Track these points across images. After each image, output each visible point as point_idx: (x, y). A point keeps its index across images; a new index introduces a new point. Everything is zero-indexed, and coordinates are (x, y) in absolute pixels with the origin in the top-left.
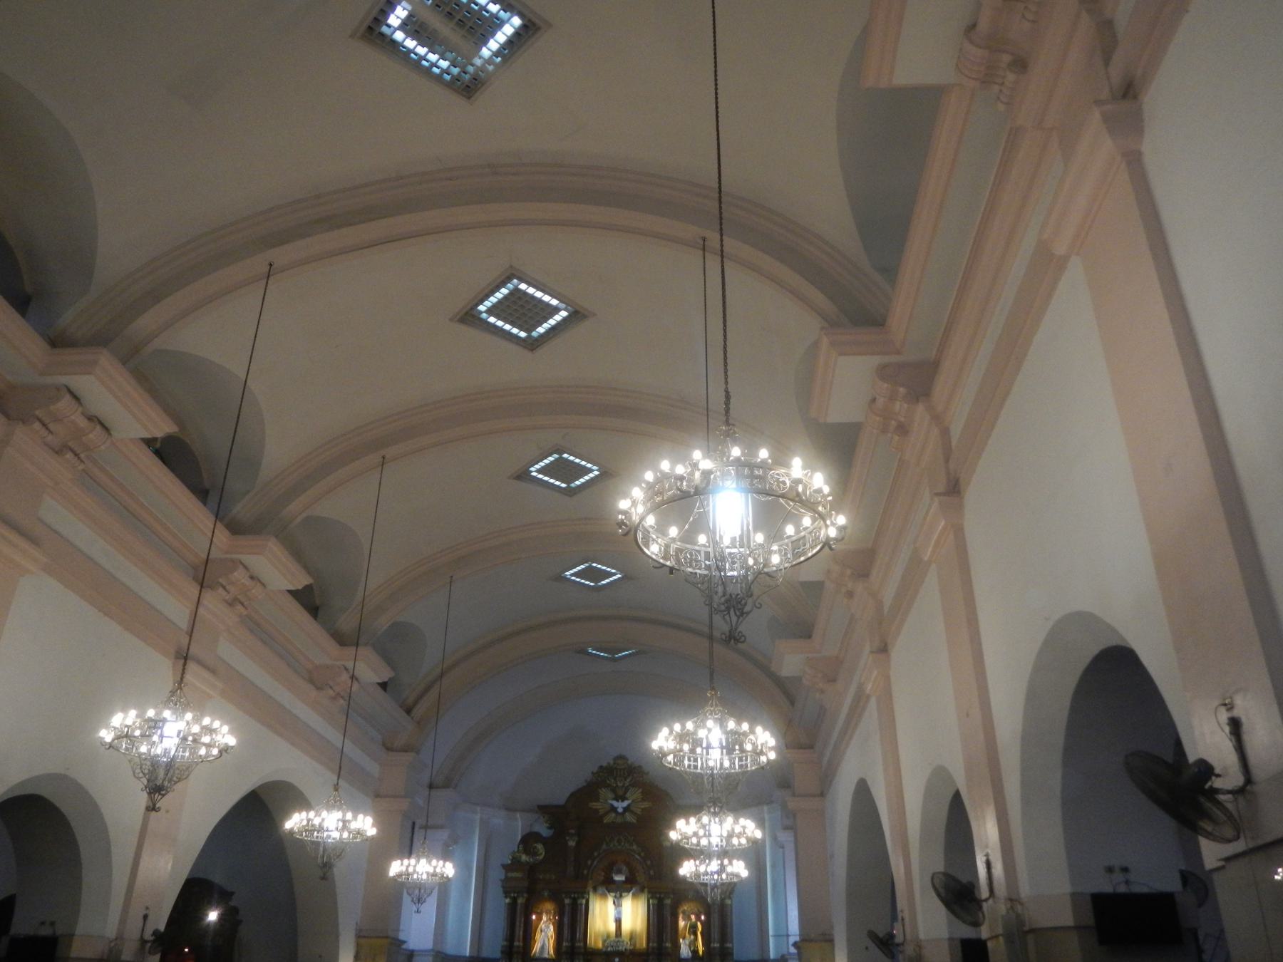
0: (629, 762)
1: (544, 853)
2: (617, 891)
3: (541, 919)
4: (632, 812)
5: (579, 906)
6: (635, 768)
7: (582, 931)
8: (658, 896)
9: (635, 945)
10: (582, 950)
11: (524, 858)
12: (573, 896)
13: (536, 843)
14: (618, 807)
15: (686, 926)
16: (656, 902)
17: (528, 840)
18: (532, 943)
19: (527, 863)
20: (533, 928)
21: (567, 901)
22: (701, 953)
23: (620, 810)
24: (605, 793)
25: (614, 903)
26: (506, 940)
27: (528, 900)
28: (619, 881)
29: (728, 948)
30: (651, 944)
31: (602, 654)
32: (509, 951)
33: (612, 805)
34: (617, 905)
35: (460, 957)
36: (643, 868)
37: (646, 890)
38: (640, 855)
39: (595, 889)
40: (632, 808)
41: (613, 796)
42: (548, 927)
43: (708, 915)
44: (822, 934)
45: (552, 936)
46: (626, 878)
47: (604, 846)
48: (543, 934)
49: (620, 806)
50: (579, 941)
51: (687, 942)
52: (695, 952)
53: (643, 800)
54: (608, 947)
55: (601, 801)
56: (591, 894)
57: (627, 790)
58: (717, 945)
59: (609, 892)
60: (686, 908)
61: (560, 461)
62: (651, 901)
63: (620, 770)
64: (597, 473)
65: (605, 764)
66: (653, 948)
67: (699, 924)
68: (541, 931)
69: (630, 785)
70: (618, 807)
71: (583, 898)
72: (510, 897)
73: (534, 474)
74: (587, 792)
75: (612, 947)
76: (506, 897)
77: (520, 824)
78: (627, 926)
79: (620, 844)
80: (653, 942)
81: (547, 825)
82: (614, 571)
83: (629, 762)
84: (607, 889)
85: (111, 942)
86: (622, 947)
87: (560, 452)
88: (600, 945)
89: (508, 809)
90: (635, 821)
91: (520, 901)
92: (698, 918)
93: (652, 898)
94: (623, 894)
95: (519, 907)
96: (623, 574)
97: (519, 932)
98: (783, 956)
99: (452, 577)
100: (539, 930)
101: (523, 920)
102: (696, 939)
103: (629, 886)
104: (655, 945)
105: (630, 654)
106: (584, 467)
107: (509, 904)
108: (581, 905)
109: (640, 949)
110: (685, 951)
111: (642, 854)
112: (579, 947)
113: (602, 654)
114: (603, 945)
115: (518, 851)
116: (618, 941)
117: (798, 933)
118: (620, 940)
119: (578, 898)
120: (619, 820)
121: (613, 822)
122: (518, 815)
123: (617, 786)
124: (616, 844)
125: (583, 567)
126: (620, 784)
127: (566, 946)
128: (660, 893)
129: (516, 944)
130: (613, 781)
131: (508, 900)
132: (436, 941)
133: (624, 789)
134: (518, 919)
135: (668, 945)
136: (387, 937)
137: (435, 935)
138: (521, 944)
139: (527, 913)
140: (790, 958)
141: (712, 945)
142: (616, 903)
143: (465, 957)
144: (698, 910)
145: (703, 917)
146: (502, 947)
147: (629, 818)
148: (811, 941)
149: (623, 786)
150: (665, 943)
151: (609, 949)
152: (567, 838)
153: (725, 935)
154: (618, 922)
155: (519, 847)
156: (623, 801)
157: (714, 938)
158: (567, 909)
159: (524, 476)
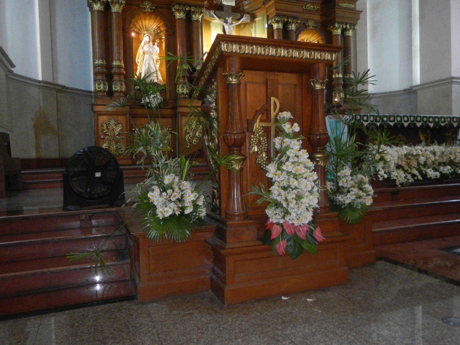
5: (195, 24)
8: (286, 20)
16: (281, 26)
20: (134, 50)
21: (179, 15)
26: (102, 58)
48: (147, 56)
58: (341, 76)
59: (219, 17)
62: (275, 26)
91: (115, 9)
93: (277, 22)
97: (117, 50)
100: (140, 51)
119: (194, 12)
138: (123, 65)
139: (125, 32)
143: (40, 82)
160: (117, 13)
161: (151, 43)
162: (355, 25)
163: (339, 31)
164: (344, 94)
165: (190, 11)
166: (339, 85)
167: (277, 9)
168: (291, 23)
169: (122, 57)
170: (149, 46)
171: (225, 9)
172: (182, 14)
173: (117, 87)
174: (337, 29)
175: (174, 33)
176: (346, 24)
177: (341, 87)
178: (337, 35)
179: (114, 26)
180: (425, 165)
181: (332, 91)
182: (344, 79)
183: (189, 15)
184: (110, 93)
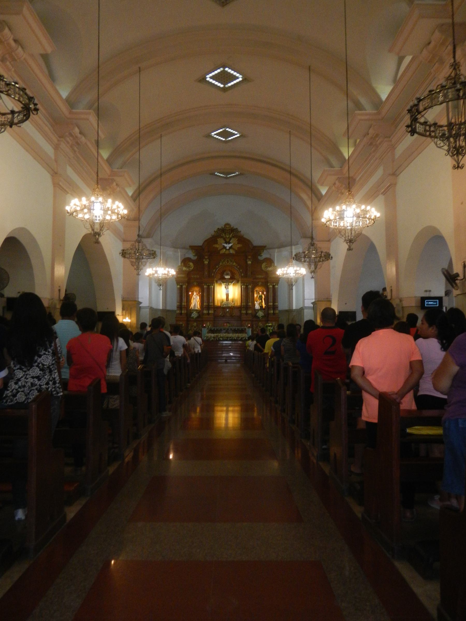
0: (232, 227)
1: (193, 267)
2: (228, 282)
3: (193, 294)
4: (234, 249)
5: (211, 289)
6: (234, 229)
7: (212, 298)
8: (246, 284)
9: (234, 304)
10: (213, 306)
11: (184, 269)
12: (208, 284)
13: (190, 262)
14: (226, 247)
15: (257, 296)
17: (185, 261)
18: (190, 303)
19: (185, 271)
20: (190, 298)
21: (205, 287)
22: (264, 307)
23: (228, 248)
24: (220, 241)
25: (225, 287)
26: (179, 302)
27: (187, 286)
28: (228, 278)
29: (276, 305)
30: (243, 304)
31: (221, 175)
32: (180, 307)
33: (224, 246)
34: (227, 288)
35: (158, 309)
36: (238, 272)
37: (240, 282)
38: (237, 267)
39: (217, 282)
40: (233, 247)
41: (224, 242)
42: (197, 297)
43: (268, 292)
44: (327, 298)
45: (198, 301)
46: (230, 277)
47: (221, 264)
49: (228, 246)
50: (211, 303)
51: (258, 303)
52: (261, 307)
53: (238, 243)
54: (223, 305)
55: (219, 244)
56: (215, 284)
57: (230, 239)
58: (271, 304)
59: (223, 283)
60: (257, 289)
61: (224, 72)
62: (242, 286)
63: (228, 230)
64: (241, 79)
65: (220, 227)
66: (244, 305)
67: (263, 296)
68: (194, 299)
69: (232, 237)
70: (226, 247)
71: (212, 285)
72: (180, 285)
73: (208, 79)
74: (212, 240)
75: (225, 305)
76: (178, 285)
77: (180, 254)
78: (230, 297)
79: (228, 263)
80: (244, 303)
81: (194, 254)
82: (236, 133)
83: (232, 227)
84: (222, 282)
85: (50, 300)
86: (230, 305)
87: (224, 67)
88: (219, 305)
89: (174, 247)
90: (235, 253)
91: (184, 286)
92: (263, 293)
93: (243, 285)
94: (230, 284)
95: (184, 289)
96: (241, 134)
97: (184, 300)
98: (302, 308)
99: (161, 134)
100: (193, 298)
101: (186, 294)
102: (262, 302)
103: (231, 280)
104: (245, 304)
105: (235, 175)
106: (235, 76)
107: (179, 288)
108: (212, 288)
109: (237, 306)
110: (257, 306)
111: (238, 267)
112: (211, 305)
113: (221, 175)
114: (221, 305)
115: (181, 266)
116: (228, 303)
117: (314, 297)
118: (229, 302)
119: (210, 285)
120: (227, 252)
121: (224, 253)
122: (179, 250)
123: (226, 237)
124: (227, 263)
125: (221, 130)
126: (228, 236)
127: (206, 305)
128: (247, 283)
129: (183, 304)
130: (224, 235)
131: (178, 286)
132: (149, 303)
133: (229, 238)
134: (184, 294)
135: (250, 304)
136: (136, 301)
137: (149, 300)
138: (186, 304)
140: (305, 309)
141: (269, 304)
142: (226, 286)
143: (160, 309)
144: (263, 290)
145: (265, 293)
146: (177, 305)
147: (232, 251)
148: (321, 301)
149: (229, 237)
150: (249, 303)
151: (224, 306)
152: (204, 260)
153: (275, 300)
154: (227, 295)
155: (181, 264)
156: (229, 243)
157: (270, 301)
158: (205, 290)
159: (203, 80)
160: (185, 288)
161: (197, 295)
162: (278, 283)
163: (271, 286)
165: (208, 285)
167: (241, 280)
168: (249, 285)
169: (185, 302)
170: (195, 297)
171: (226, 279)
172: (206, 286)
173: (183, 312)
174: (270, 285)
175: (204, 292)
176: (274, 283)
178: (270, 288)
179: (183, 291)
180: (220, 337)
182: (274, 305)
183: (209, 286)
184: (181, 314)
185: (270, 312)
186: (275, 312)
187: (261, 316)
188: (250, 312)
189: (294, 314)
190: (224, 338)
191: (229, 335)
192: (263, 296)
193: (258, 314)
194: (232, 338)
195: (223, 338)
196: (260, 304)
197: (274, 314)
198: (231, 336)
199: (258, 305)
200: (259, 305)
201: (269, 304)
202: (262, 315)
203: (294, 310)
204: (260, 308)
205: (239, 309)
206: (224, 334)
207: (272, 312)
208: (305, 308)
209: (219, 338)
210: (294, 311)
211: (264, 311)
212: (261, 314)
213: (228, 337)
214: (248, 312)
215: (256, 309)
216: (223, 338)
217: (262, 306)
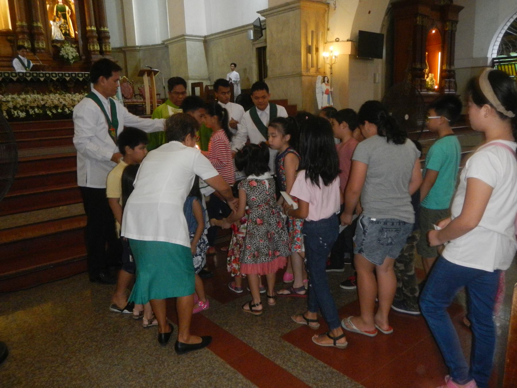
22: (73, 35)
29: (105, 32)
30: (18, 23)
51: (58, 25)
52: (67, 35)
58: (94, 28)
66: (22, 27)
80: (21, 21)
102: (66, 23)
104: (24, 24)
110: (56, 33)
135: (40, 24)
140: (188, 41)
141: (88, 28)
164: (99, 47)
166: (93, 37)
177: (95, 40)
180: (15, 108)
181: (88, 43)
182: (99, 32)
185: (94, 48)
186: (104, 49)
187: (74, 58)
188: (42, 45)
189: (140, 55)
190: (31, 112)
191: (45, 97)
192: (67, 8)
193: (63, 52)
194: (63, 109)
195: (24, 108)
196: (64, 28)
197: (101, 52)
198: (56, 102)
199: (59, 30)
200: (61, 30)
201: (88, 28)
202: (74, 55)
203: (138, 48)
204: (65, 39)
205: (9, 38)
206: (30, 97)
207: (97, 47)
208: (168, 42)
209: (9, 112)
210: (139, 51)
211: (76, 47)
212: (72, 52)
213: (43, 107)
214: (36, 46)
215: (57, 39)
216: (27, 112)
217: (69, 34)
